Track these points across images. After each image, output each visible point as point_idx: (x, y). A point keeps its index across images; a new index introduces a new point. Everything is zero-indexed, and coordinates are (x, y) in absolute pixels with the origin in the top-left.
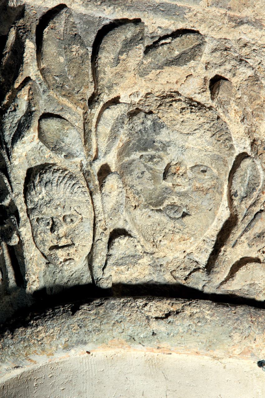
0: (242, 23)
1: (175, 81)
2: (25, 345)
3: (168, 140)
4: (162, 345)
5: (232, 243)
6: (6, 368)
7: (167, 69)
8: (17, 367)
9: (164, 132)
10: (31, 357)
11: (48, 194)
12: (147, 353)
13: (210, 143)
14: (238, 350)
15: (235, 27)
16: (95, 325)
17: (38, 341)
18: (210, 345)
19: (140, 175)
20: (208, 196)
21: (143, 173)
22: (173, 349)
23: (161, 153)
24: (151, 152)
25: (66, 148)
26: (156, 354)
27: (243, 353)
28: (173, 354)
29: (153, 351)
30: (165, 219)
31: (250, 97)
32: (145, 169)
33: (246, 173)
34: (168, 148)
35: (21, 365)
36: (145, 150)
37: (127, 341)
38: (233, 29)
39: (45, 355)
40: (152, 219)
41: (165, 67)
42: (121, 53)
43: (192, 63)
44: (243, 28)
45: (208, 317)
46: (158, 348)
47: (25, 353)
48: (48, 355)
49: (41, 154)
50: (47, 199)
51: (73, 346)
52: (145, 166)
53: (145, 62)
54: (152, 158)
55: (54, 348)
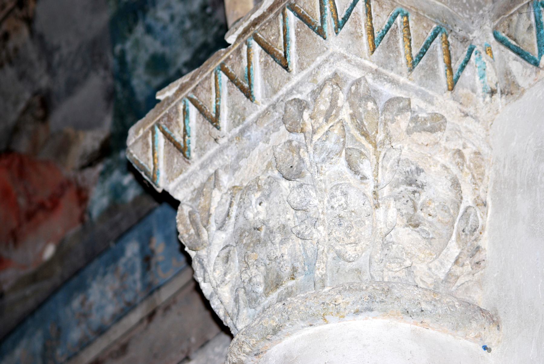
0: (467, 115)
1: (426, 144)
2: (324, 307)
3: (425, 181)
4: (425, 321)
5: (461, 264)
6: (303, 325)
7: (423, 133)
8: (311, 325)
9: (422, 174)
10: (326, 317)
11: (346, 202)
12: (412, 325)
13: (451, 191)
14: (473, 334)
15: (463, 117)
16: (381, 298)
17: (336, 305)
18: (456, 328)
19: (405, 202)
20: (447, 227)
21: (407, 201)
22: (431, 325)
23: (420, 190)
24: (414, 188)
25: (361, 171)
26: (419, 327)
27: (476, 337)
28: (430, 329)
29: (417, 325)
30: (419, 237)
31: (475, 165)
32: (409, 199)
33: (469, 217)
34: (425, 187)
35: (315, 324)
36: (410, 185)
37: (403, 313)
38: (462, 118)
39: (338, 317)
40: (411, 236)
41: (423, 132)
42: (397, 115)
43: (439, 134)
44: (468, 118)
45: (457, 306)
46: (422, 322)
47: (323, 313)
48: (340, 317)
49: (340, 175)
50: (345, 206)
51: (361, 312)
52: (409, 197)
53: (410, 125)
54: (414, 192)
55: (347, 311)
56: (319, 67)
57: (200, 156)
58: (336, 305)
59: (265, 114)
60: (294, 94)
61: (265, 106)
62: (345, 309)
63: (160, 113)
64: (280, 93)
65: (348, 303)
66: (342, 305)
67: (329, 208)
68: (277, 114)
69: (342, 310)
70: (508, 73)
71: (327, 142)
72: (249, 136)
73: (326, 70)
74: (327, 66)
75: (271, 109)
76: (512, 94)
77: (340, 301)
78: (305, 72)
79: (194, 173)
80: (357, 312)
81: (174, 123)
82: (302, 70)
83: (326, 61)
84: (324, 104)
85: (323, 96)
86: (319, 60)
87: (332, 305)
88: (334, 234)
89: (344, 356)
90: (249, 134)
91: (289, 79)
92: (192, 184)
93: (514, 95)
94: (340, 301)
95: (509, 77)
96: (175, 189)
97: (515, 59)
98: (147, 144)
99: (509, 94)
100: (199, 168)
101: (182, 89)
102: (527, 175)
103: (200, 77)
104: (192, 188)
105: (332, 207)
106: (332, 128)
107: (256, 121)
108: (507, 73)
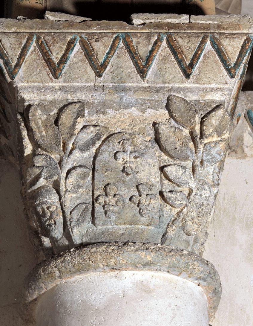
8: (169, 272)
39: (188, 276)
56: (212, 90)
57: (65, 81)
58: (193, 268)
59: (147, 90)
60: (180, 93)
61: (147, 85)
62: (196, 273)
63: (41, 29)
64: (167, 85)
65: (199, 270)
66: (196, 270)
67: (199, 195)
68: (157, 97)
69: (194, 273)
70: (241, 139)
71: (213, 149)
72: (123, 96)
73: (217, 95)
74: (220, 93)
75: (153, 90)
76: (236, 153)
77: (196, 267)
78: (197, 85)
79: (53, 89)
80: (199, 279)
81: (57, 46)
82: (197, 83)
83: (221, 90)
84: (215, 121)
85: (216, 114)
86: (214, 85)
87: (191, 267)
88: (193, 213)
89: (185, 305)
90: (123, 94)
91: (182, 82)
92: (45, 96)
93: (238, 155)
94: (196, 267)
95: (240, 142)
96: (26, 88)
97: (249, 134)
98: (20, 44)
99: (234, 152)
100: (57, 87)
101: (71, 24)
102: (245, 216)
103: (96, 29)
104: (43, 98)
105: (201, 195)
106: (220, 142)
107: (137, 90)
108: (240, 139)
